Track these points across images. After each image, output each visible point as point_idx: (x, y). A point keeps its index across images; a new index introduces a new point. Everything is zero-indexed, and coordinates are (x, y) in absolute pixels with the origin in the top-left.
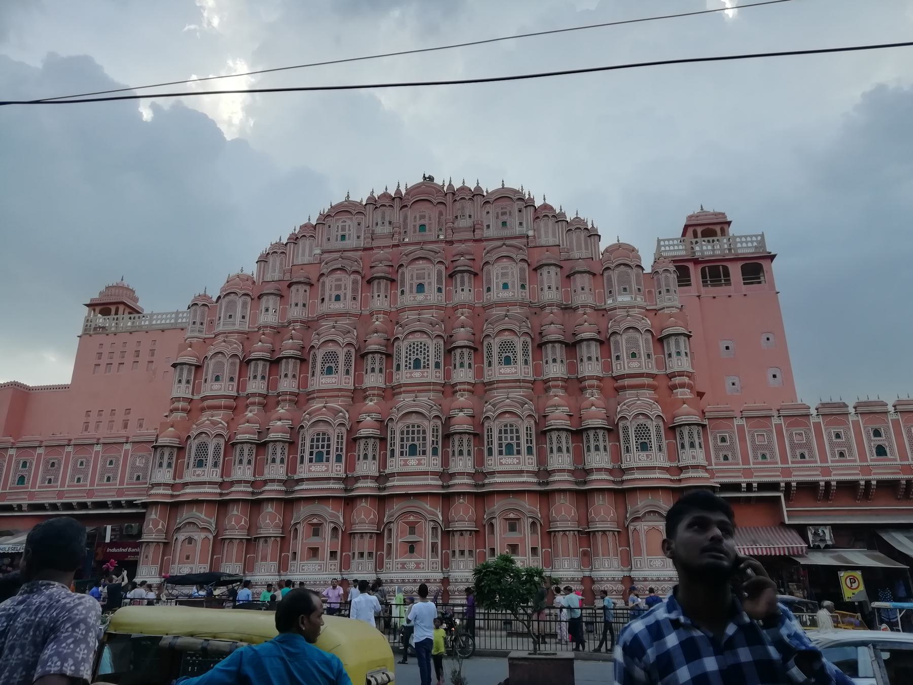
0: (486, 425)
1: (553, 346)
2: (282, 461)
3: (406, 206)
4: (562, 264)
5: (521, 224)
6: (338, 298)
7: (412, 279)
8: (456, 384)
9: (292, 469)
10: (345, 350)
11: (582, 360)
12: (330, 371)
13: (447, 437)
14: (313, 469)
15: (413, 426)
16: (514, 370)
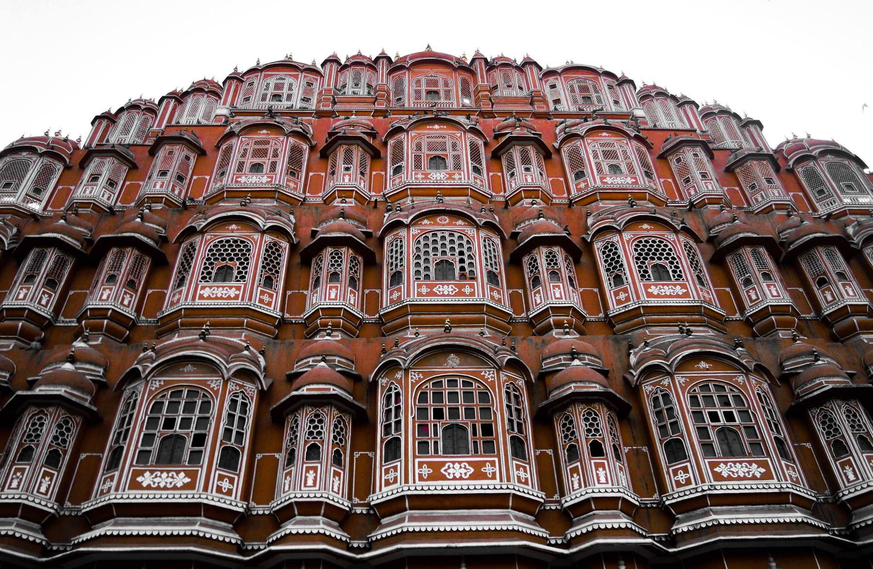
0: (647, 388)
1: (755, 253)
2: (53, 459)
3: (402, 68)
4: (714, 152)
5: (616, 102)
6: (257, 168)
7: (419, 147)
8: (544, 314)
9: (76, 484)
10: (268, 238)
11: (822, 282)
12: (224, 274)
13: (544, 419)
14: (146, 479)
15: (452, 383)
16: (679, 290)
